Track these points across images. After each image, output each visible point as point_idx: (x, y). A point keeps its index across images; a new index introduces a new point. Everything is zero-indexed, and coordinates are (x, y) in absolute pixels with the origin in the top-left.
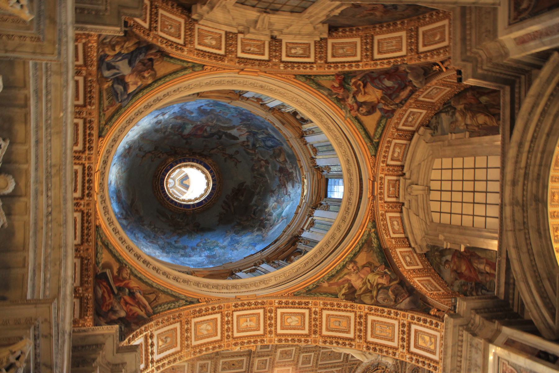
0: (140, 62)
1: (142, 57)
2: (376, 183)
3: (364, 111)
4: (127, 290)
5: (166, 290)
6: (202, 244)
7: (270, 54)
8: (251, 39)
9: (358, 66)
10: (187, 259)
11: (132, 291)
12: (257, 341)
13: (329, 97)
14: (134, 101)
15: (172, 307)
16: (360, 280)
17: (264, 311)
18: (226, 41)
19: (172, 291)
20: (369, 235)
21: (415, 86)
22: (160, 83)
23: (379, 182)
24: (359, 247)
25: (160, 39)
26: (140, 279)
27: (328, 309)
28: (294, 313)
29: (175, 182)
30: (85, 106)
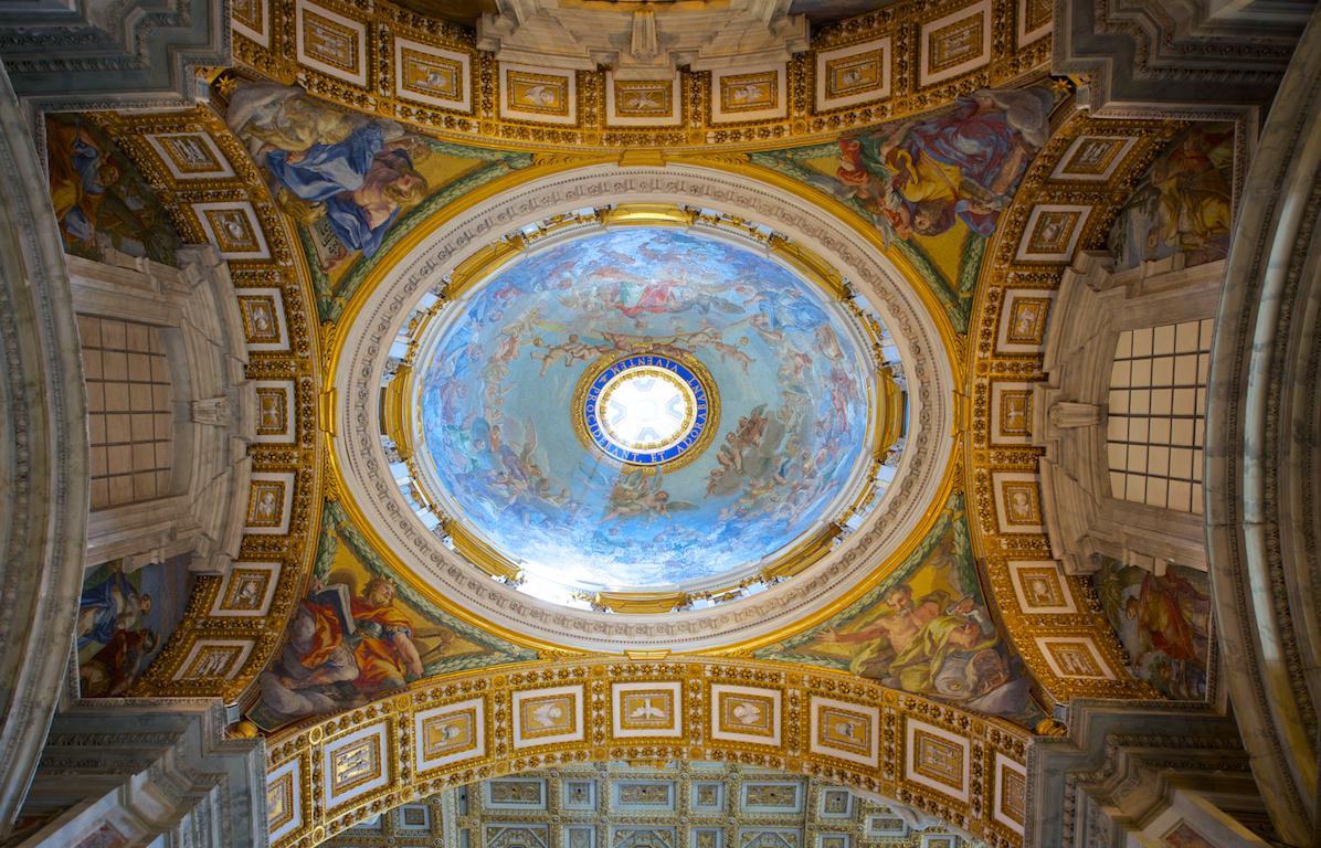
0: (375, 160)
2: (966, 400)
3: (927, 224)
7: (684, 111)
8: (638, 82)
9: (883, 112)
13: (839, 198)
14: (391, 244)
16: (913, 631)
18: (578, 93)
20: (949, 525)
21: (1031, 145)
22: (441, 201)
23: (974, 396)
24: (920, 554)
25: (399, 108)
30: (273, 261)
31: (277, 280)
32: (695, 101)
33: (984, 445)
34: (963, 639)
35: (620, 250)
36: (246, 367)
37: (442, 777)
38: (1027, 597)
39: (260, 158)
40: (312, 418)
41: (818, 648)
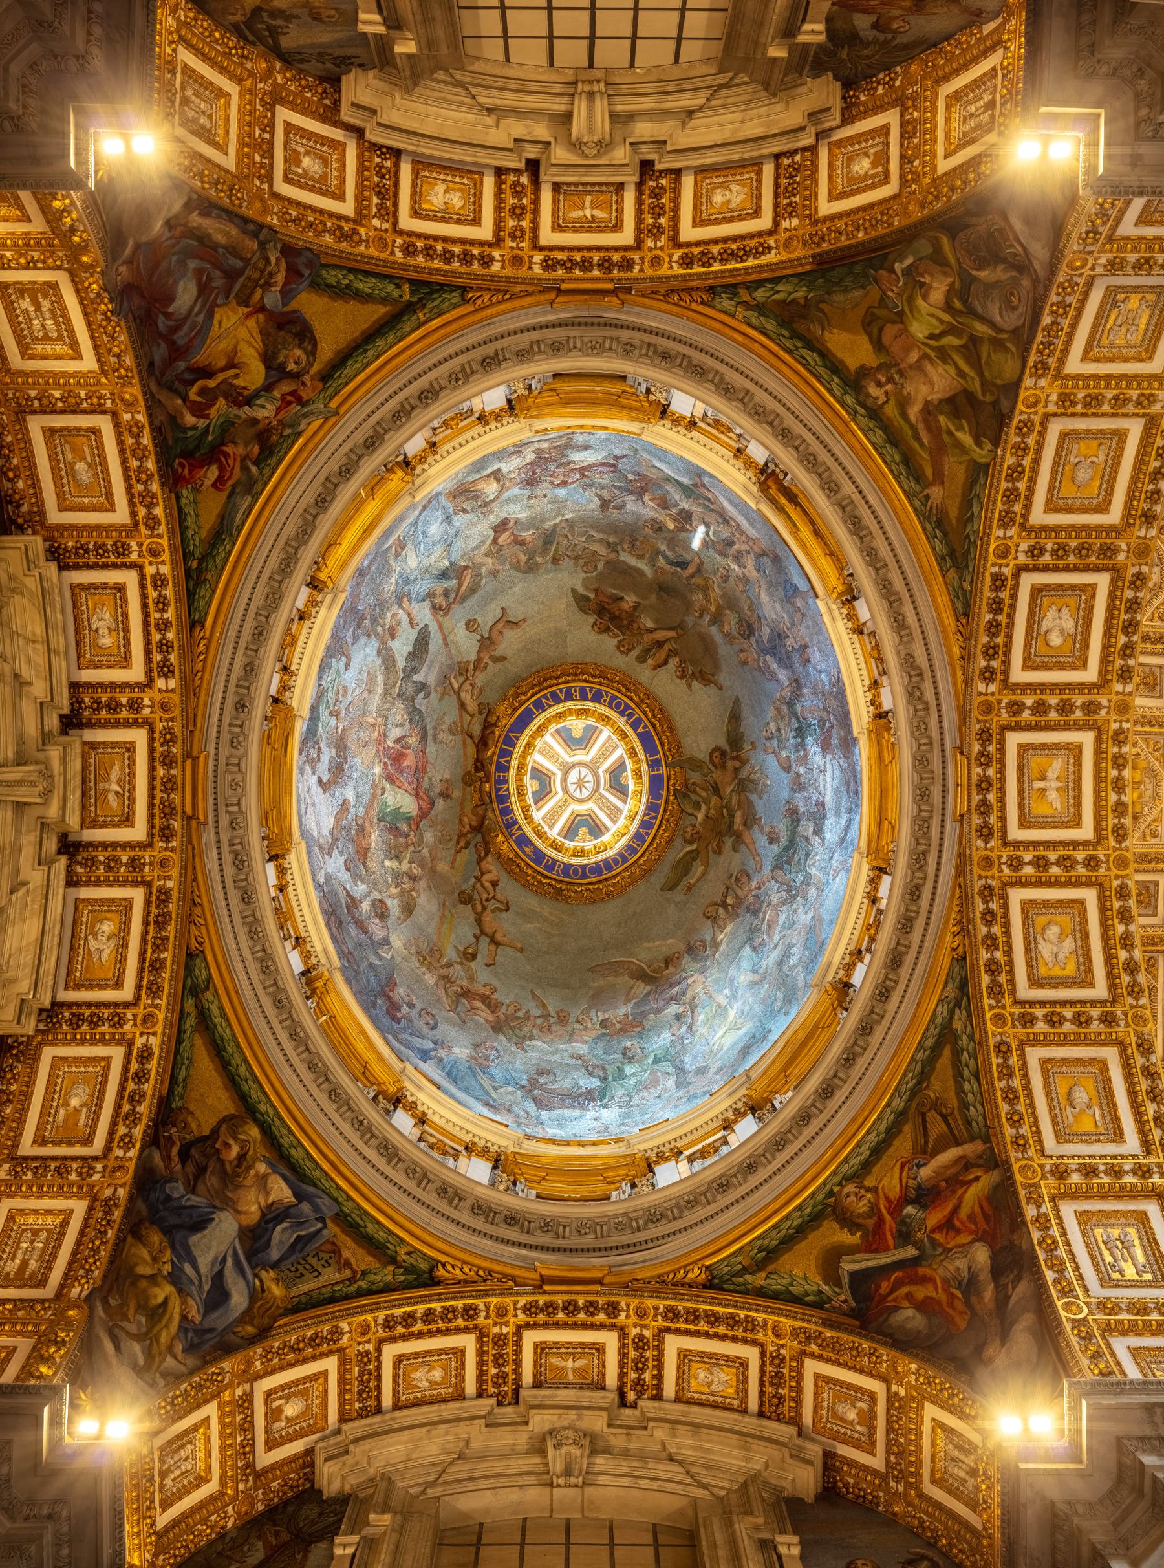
0: (193, 1191)
1: (177, 1190)
2: (564, 286)
3: (298, 352)
4: (910, 1210)
5: (918, 1068)
6: (784, 754)
7: (127, 724)
10: (830, 821)
11: (912, 1194)
12: (1115, 757)
13: (258, 487)
14: (317, 1174)
15: (972, 1063)
17: (1013, 729)
19: (920, 1046)
22: (255, 1095)
23: (560, 272)
25: (119, 1153)
26: (878, 1151)
27: (1027, 508)
28: (1030, 622)
29: (575, 765)
31: (370, 1347)
32: (114, 707)
33: (636, 257)
34: (939, 290)
35: (328, 823)
36: (500, 1404)
37: (1151, 1113)
38: (874, 186)
39: (191, 1362)
40: (581, 1302)
41: (953, 512)
